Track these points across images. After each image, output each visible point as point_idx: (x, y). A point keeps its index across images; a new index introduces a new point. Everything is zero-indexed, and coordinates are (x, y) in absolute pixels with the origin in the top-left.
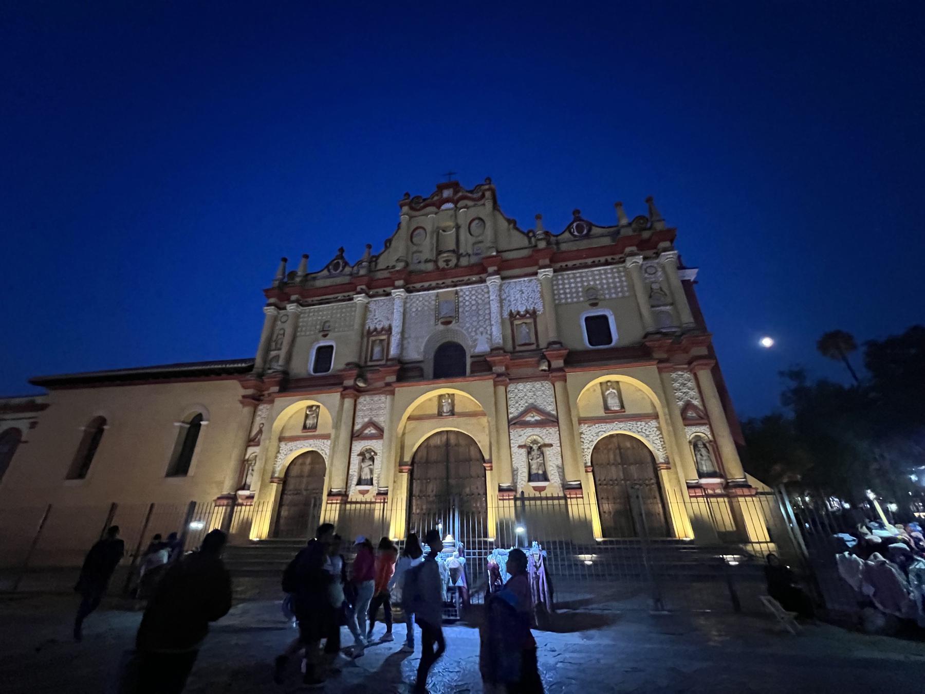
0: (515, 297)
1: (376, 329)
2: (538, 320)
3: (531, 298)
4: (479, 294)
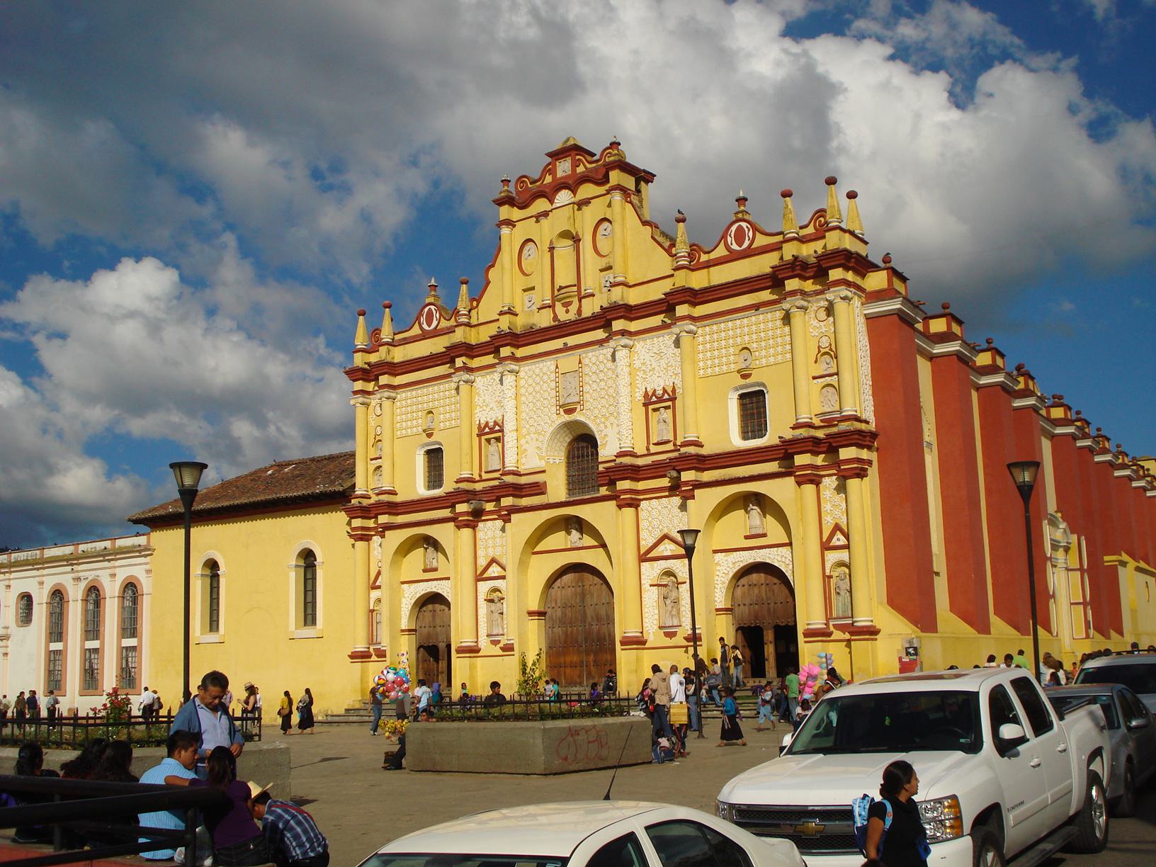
0: (651, 365)
1: (487, 424)
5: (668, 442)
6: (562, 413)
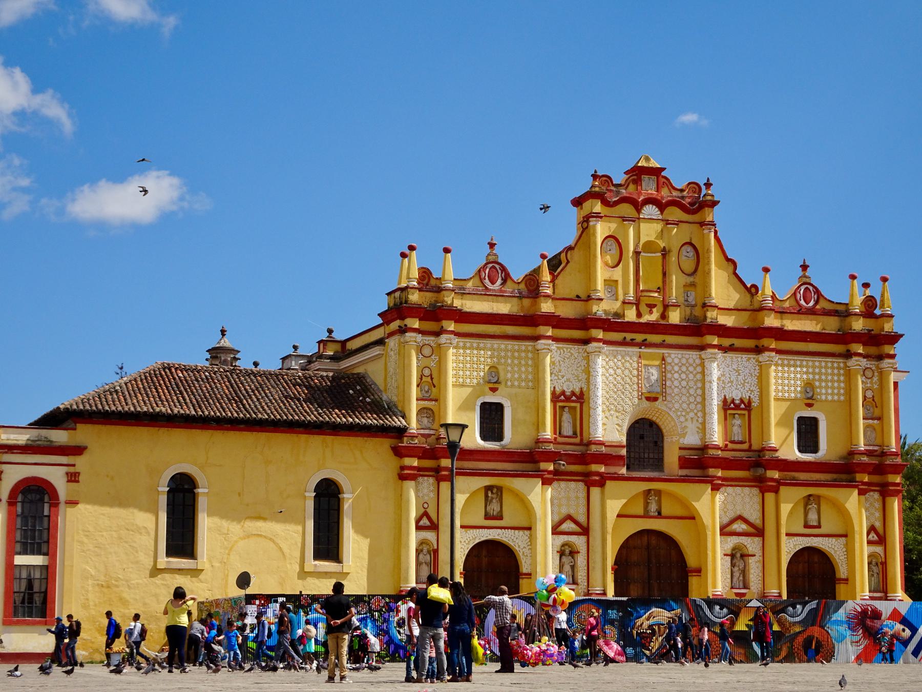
1: (563, 393)
2: (753, 413)
3: (748, 383)
4: (691, 365)
5: (741, 442)
6: (644, 399)
